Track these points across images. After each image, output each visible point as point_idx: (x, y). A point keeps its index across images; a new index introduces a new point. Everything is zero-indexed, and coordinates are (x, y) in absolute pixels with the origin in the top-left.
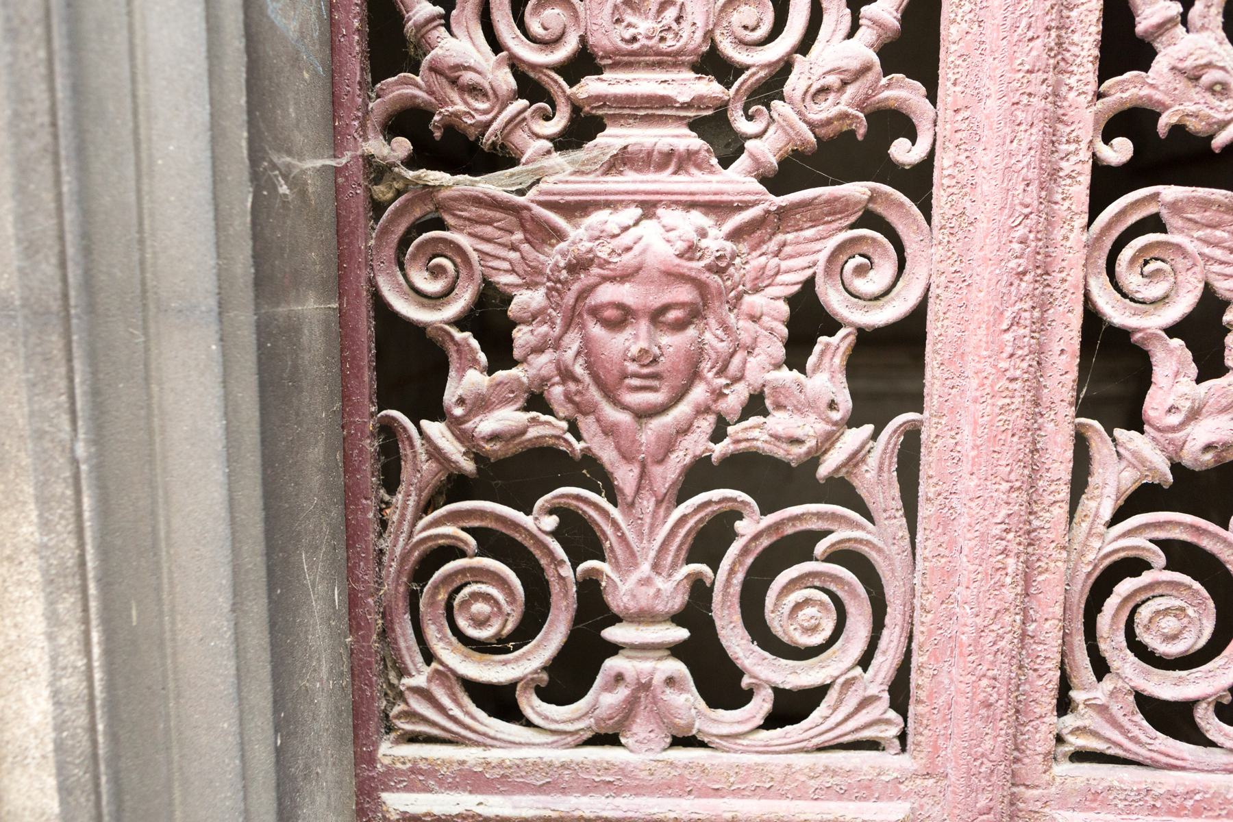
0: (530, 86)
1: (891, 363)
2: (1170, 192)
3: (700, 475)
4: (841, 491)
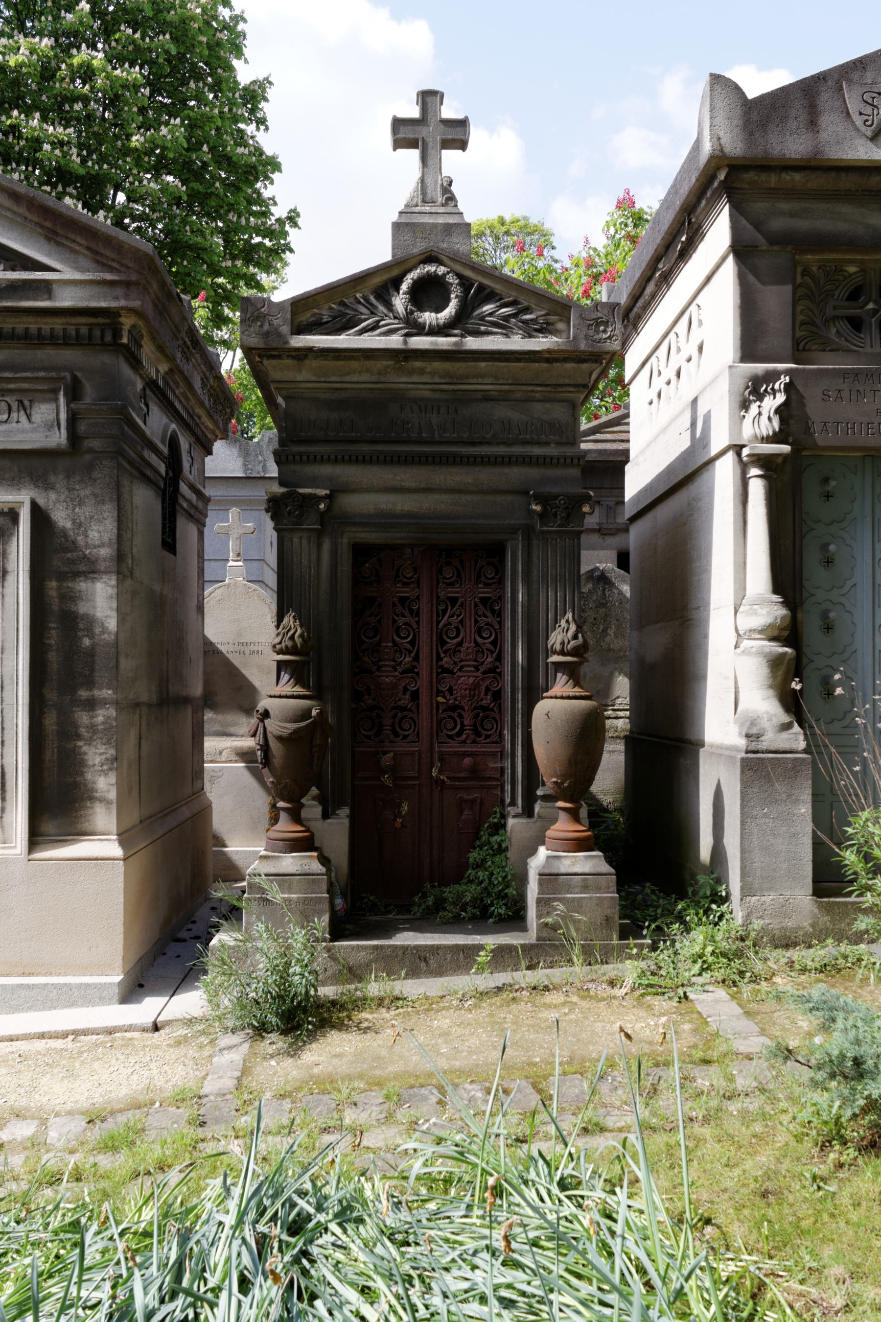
0: (373, 662)
1: (415, 695)
3: (393, 708)
4: (410, 710)
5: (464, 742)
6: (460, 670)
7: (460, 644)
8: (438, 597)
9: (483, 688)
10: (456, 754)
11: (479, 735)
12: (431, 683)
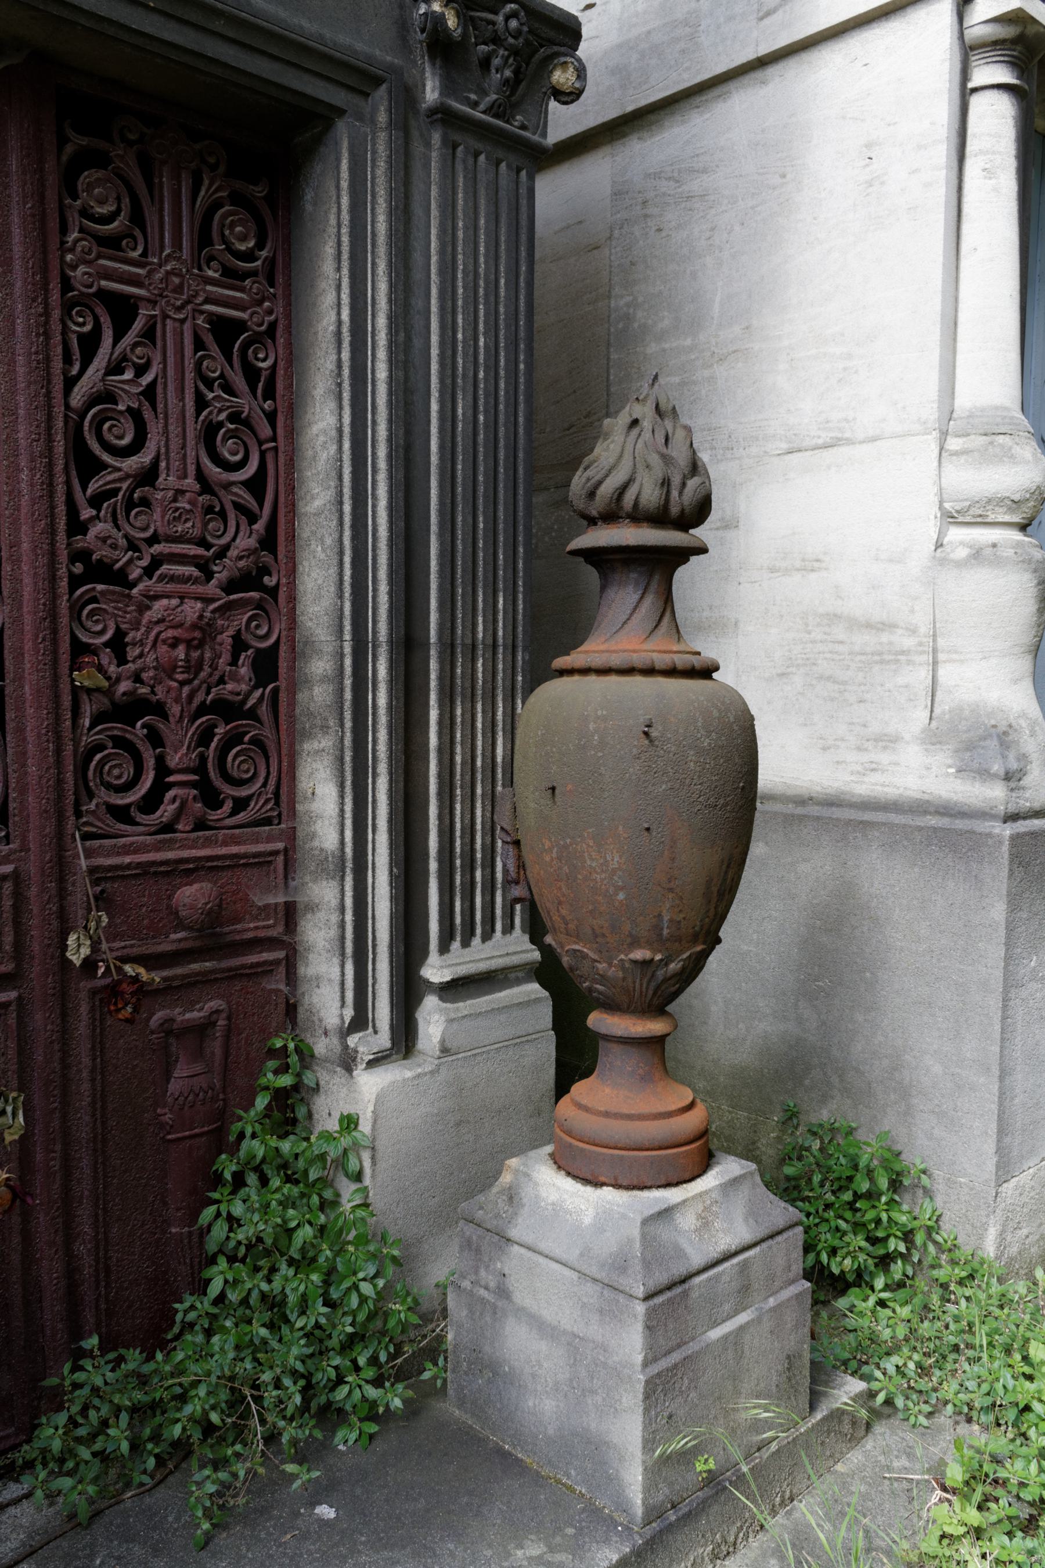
2: (100, 587)
5: (168, 828)
6: (149, 572)
7: (149, 476)
8: (66, 285)
9: (226, 638)
10: (146, 871)
11: (212, 799)
12: (53, 614)
